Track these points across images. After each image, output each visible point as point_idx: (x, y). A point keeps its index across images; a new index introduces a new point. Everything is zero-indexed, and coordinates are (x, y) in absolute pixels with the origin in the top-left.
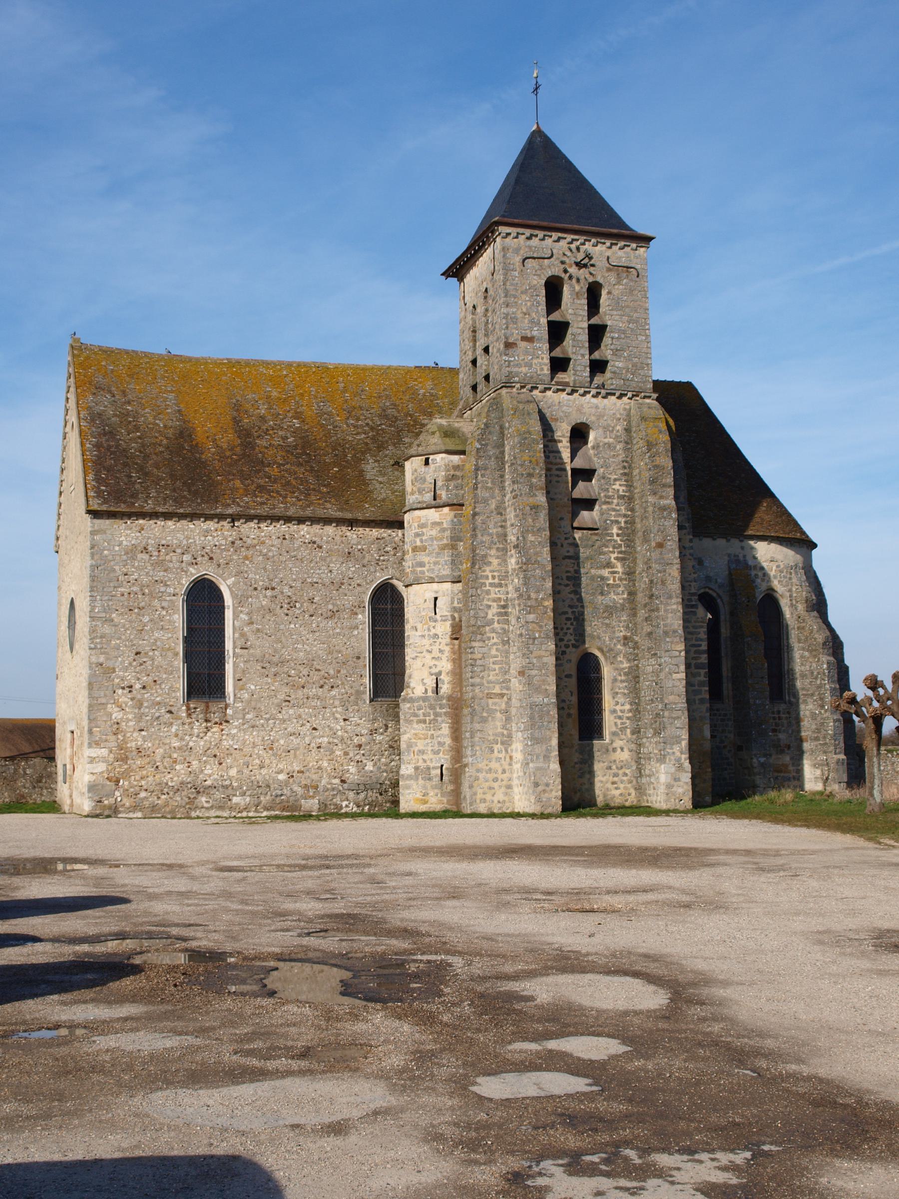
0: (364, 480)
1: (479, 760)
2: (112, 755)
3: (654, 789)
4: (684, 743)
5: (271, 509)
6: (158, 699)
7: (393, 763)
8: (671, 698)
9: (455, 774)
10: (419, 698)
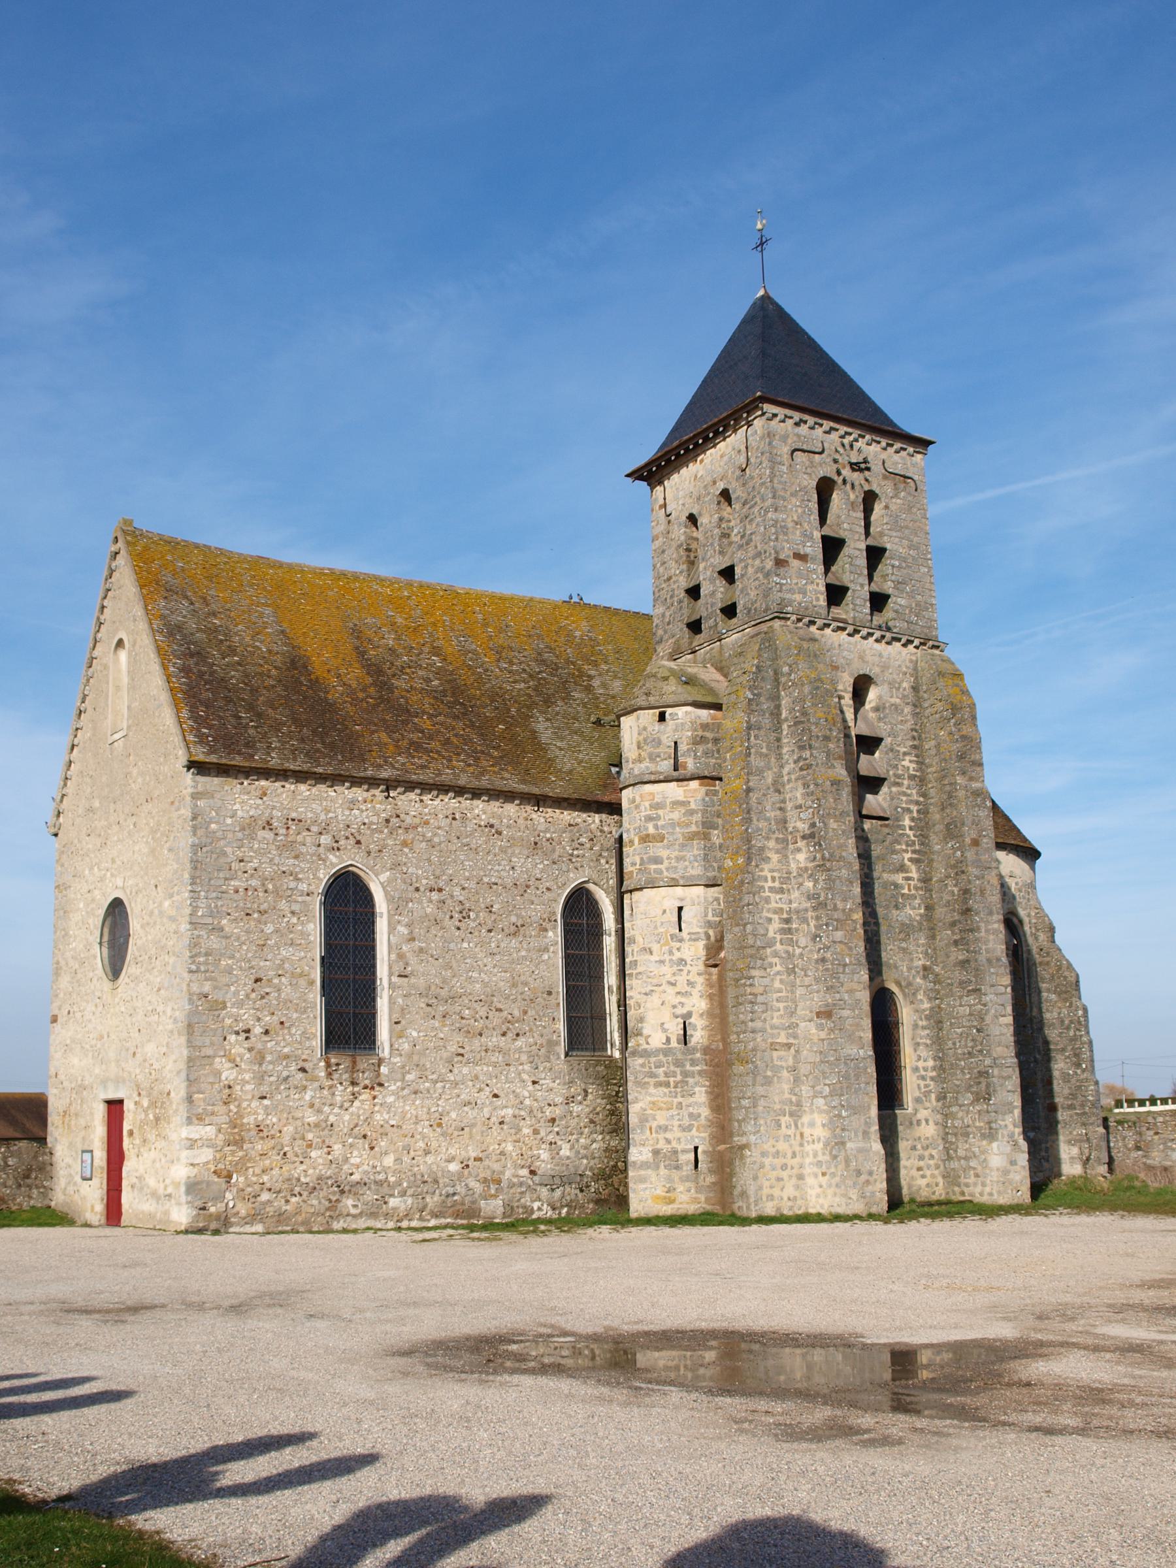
0: (539, 743)
1: (764, 1139)
2: (221, 1136)
3: (977, 1176)
4: (1017, 1112)
5: (437, 775)
6: (286, 1050)
7: (594, 1146)
8: (999, 1049)
9: (723, 1160)
10: (658, 1051)
